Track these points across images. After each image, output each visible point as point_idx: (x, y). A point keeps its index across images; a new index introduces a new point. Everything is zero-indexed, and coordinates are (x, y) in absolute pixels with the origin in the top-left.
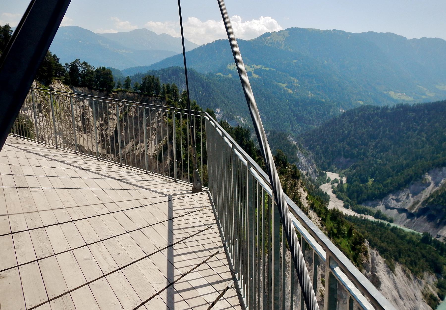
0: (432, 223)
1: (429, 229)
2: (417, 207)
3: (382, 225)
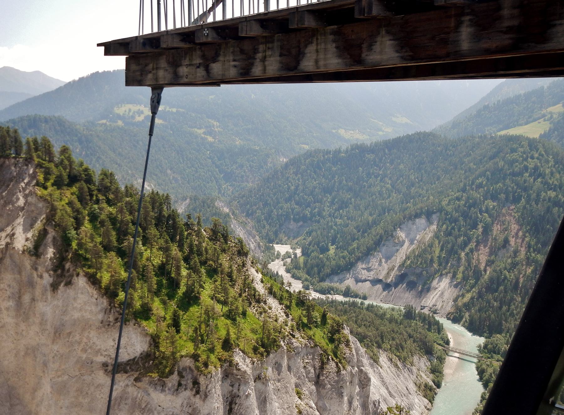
0: (413, 292)
1: (411, 301)
2: (393, 274)
3: (354, 304)
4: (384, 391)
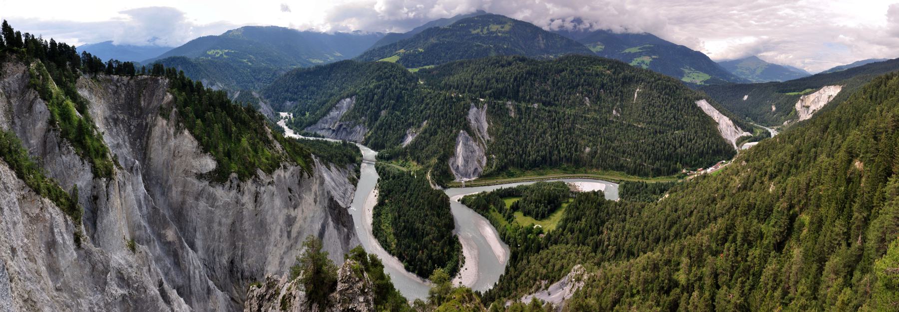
4: (333, 184)
